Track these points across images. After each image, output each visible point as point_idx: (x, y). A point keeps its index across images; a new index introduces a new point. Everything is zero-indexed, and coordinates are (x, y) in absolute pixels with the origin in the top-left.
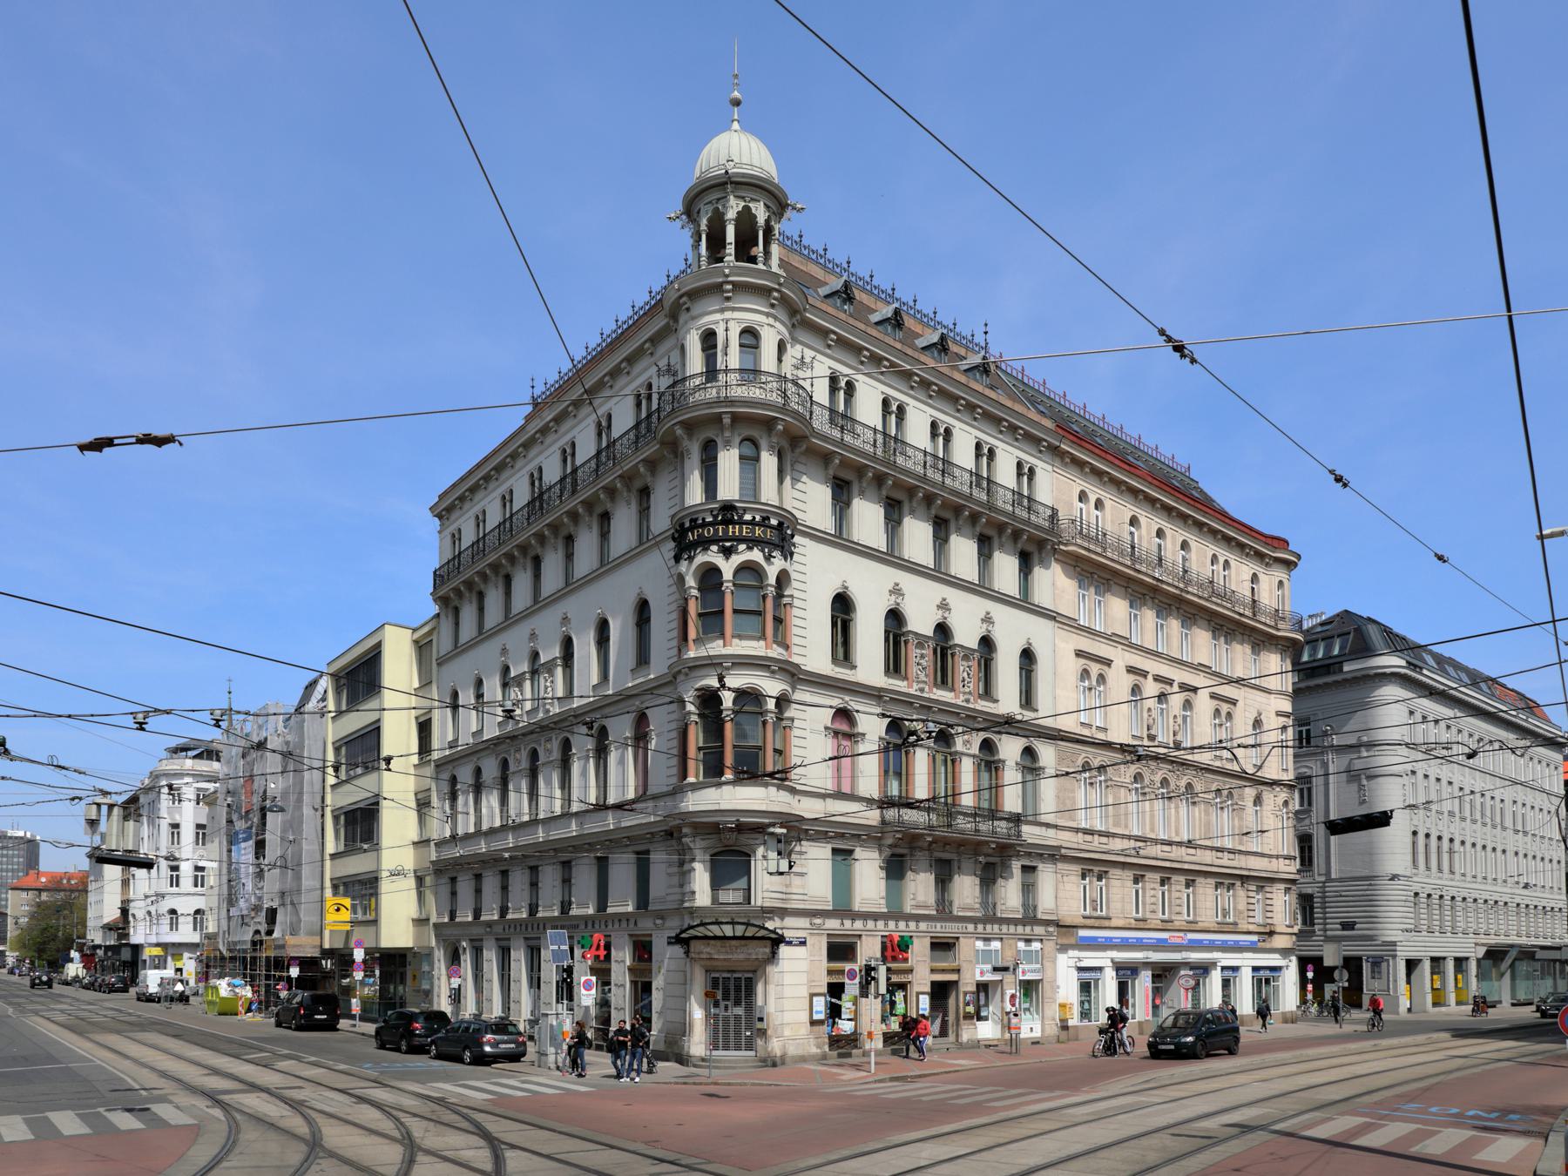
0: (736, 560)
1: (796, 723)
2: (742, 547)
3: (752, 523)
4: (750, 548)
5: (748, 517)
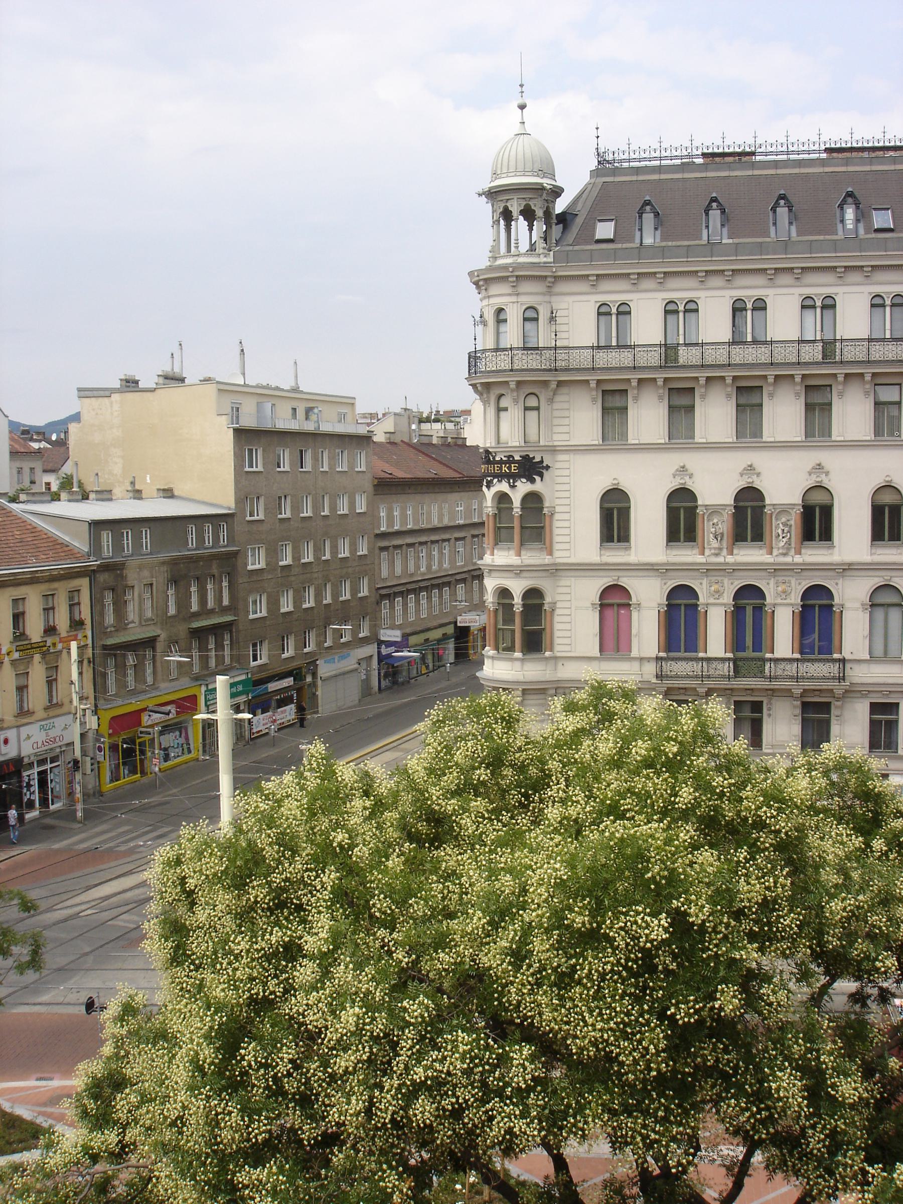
0: (494, 490)
1: (559, 605)
2: (496, 480)
3: (501, 462)
4: (499, 481)
5: (497, 459)
